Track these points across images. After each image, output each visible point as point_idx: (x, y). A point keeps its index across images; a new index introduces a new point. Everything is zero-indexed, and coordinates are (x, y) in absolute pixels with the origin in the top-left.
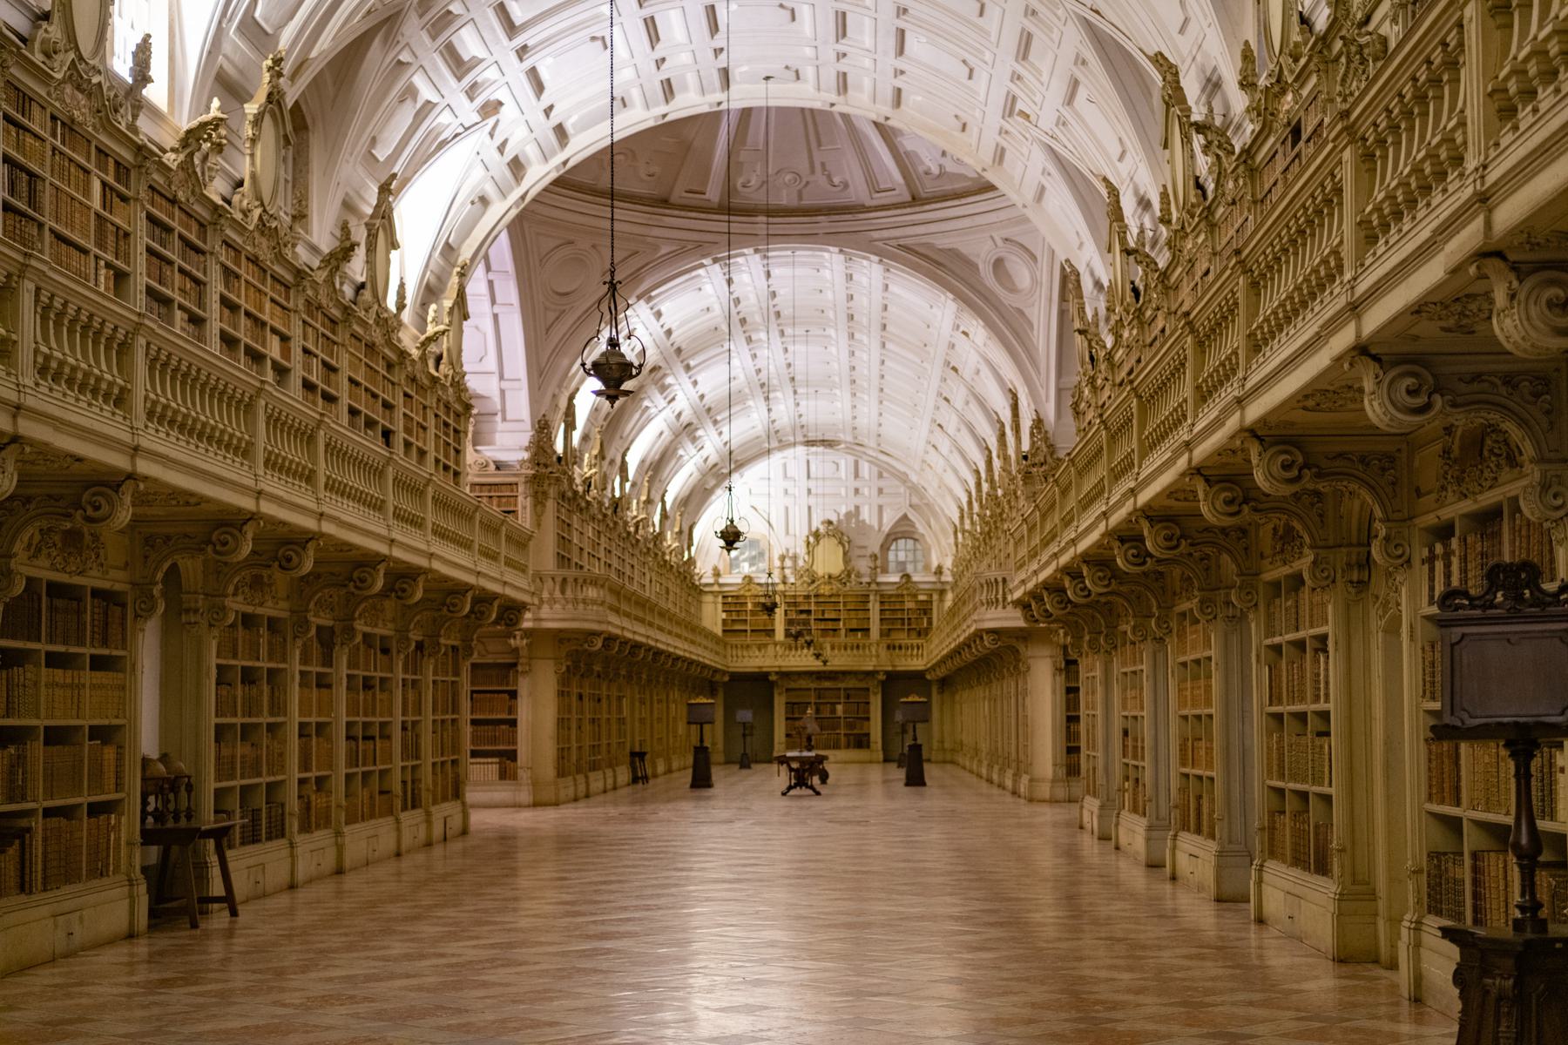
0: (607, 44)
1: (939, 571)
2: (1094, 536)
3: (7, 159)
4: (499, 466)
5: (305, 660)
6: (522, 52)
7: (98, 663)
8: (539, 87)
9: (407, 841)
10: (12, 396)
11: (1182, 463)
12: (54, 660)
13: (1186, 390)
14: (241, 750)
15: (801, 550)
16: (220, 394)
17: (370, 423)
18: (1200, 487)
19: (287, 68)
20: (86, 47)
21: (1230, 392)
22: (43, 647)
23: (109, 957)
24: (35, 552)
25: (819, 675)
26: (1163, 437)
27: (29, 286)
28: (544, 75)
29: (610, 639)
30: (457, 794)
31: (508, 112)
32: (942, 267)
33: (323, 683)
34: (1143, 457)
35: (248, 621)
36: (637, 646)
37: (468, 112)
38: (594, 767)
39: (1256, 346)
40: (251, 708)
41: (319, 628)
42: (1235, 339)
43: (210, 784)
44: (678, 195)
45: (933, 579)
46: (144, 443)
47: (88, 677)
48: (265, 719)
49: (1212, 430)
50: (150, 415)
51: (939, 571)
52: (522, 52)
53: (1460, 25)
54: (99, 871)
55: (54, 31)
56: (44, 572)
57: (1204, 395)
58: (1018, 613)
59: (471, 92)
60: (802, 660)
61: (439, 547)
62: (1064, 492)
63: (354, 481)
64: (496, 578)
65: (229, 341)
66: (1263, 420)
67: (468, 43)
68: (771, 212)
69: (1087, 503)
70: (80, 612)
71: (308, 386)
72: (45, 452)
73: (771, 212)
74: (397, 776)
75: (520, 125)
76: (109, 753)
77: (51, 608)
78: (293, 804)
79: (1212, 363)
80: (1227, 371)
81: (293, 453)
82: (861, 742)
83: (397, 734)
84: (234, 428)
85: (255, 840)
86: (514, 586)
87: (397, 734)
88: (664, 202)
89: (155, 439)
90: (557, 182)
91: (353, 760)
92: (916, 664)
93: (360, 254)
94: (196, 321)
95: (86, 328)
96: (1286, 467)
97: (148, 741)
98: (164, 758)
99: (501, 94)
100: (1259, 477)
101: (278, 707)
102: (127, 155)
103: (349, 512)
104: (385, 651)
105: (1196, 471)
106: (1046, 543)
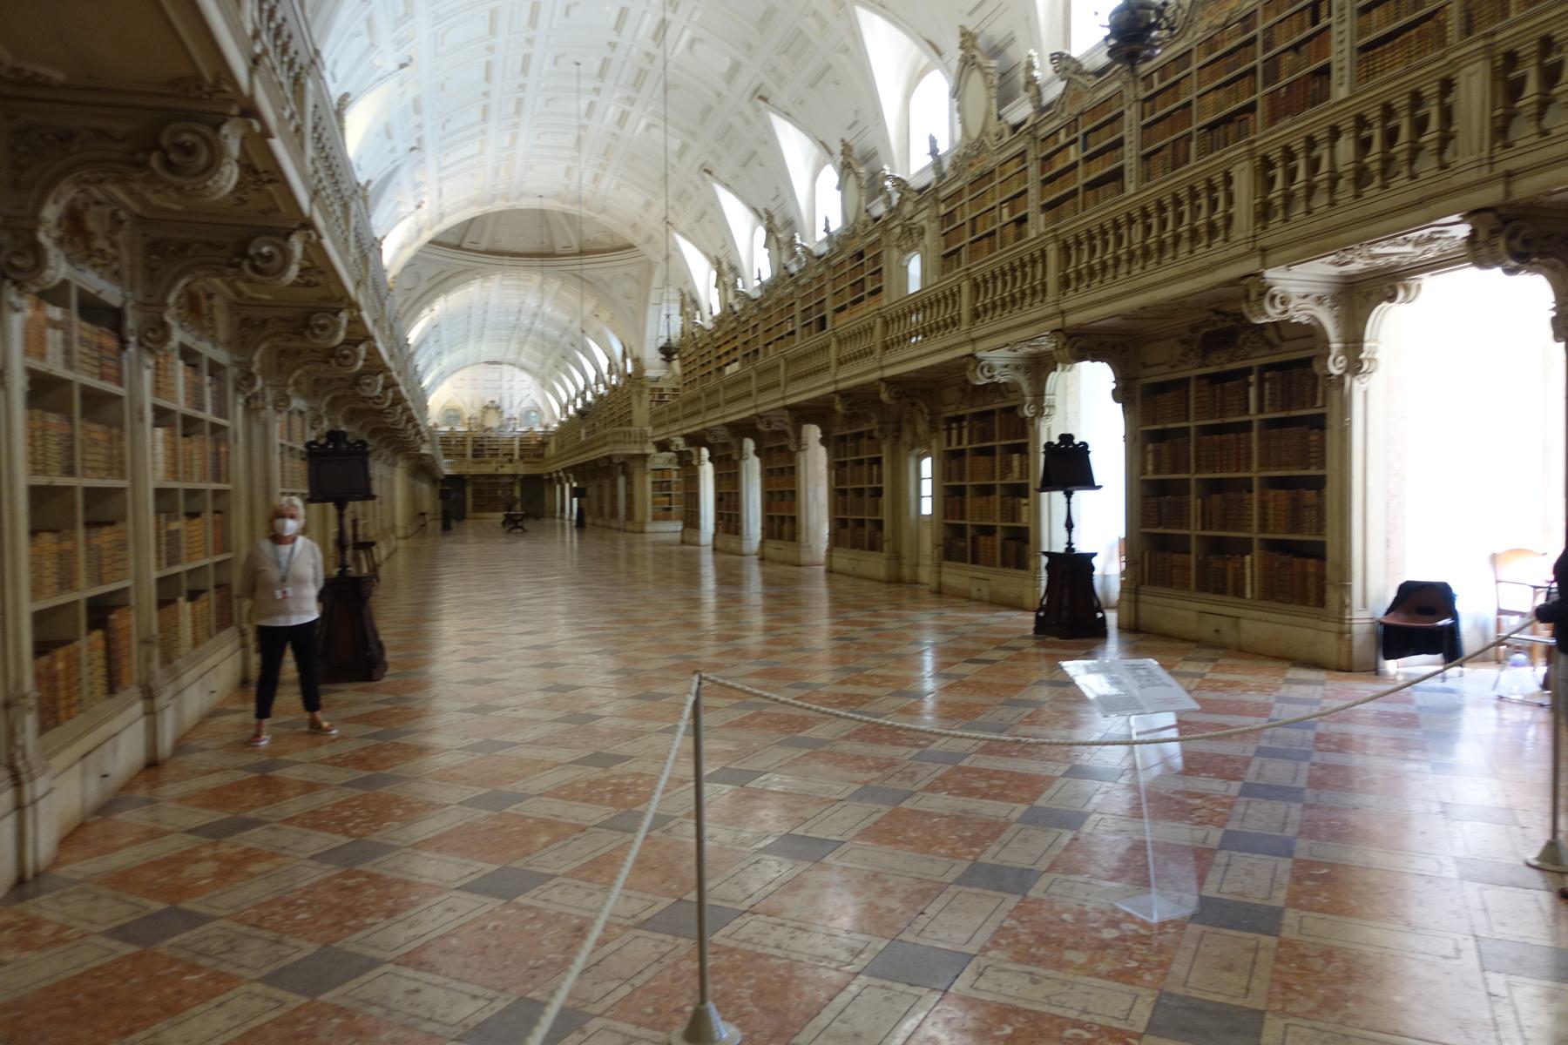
6: (441, 179)
8: (440, 195)
11: (831, 389)
15: (477, 414)
18: (837, 399)
31: (425, 206)
32: (586, 283)
39: (886, 347)
49: (853, 376)
52: (441, 179)
53: (1043, 252)
57: (840, 363)
59: (415, 197)
75: (424, 215)
79: (849, 349)
88: (458, 247)
90: (432, 242)
92: (537, 471)
99: (425, 199)
100: (884, 396)
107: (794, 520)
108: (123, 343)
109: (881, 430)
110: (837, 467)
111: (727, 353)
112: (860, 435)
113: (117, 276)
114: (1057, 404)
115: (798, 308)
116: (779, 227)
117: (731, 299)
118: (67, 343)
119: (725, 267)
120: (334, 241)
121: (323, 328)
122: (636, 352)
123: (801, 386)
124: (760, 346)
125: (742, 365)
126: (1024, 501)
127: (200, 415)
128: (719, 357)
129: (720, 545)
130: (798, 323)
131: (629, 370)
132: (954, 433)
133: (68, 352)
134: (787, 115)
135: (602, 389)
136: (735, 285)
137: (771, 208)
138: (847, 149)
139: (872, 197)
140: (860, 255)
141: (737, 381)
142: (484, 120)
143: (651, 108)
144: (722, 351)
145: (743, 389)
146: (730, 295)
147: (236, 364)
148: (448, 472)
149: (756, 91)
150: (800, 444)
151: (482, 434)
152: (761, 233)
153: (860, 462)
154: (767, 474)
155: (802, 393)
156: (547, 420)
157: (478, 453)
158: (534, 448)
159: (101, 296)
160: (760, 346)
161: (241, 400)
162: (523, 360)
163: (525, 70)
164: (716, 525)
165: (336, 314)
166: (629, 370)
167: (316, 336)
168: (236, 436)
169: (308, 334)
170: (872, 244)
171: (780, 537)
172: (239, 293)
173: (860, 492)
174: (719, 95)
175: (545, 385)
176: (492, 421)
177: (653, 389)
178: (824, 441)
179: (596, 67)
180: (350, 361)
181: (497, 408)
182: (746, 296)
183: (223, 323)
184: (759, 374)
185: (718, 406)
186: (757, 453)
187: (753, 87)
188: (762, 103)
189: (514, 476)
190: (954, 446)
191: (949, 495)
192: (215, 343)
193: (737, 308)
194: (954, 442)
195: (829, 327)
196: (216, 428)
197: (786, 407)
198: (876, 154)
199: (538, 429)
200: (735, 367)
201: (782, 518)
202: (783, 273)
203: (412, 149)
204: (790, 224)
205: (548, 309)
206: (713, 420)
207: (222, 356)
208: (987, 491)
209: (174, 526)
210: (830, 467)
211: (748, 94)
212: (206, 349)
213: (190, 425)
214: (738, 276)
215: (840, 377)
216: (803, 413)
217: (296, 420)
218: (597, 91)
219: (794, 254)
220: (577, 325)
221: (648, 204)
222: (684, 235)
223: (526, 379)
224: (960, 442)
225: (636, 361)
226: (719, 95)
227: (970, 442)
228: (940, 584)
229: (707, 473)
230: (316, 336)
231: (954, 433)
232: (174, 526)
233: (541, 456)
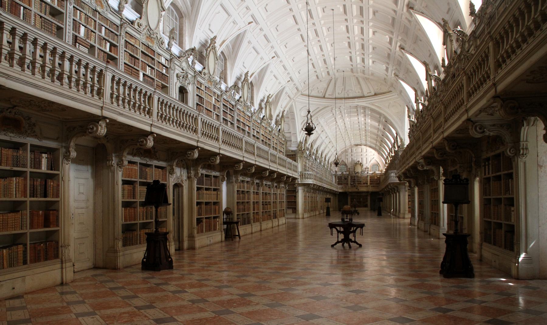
1: (381, 171)
2: (413, 163)
3: (197, 95)
4: (292, 151)
5: (254, 189)
7: (215, 190)
9: (274, 225)
10: (197, 139)
11: (431, 146)
12: (207, 189)
13: (432, 131)
14: (241, 207)
16: (236, 137)
17: (266, 143)
18: (435, 151)
19: (249, 75)
20: (211, 73)
21: (441, 130)
22: (204, 187)
23: (217, 245)
24: (203, 168)
26: (427, 141)
27: (200, 118)
29: (314, 185)
30: (284, 216)
33: (257, 193)
34: (423, 145)
35: (243, 181)
36: (320, 186)
38: (312, 211)
40: (244, 198)
41: (257, 183)
42: (442, 119)
43: (236, 213)
46: (221, 147)
47: (213, 192)
48: (246, 201)
49: (437, 139)
50: (223, 142)
51: (381, 171)
54: (215, 230)
55: (206, 71)
56: (204, 172)
57: (435, 132)
58: (397, 179)
60: (355, 190)
61: (279, 167)
62: (407, 154)
63: (262, 154)
64: (290, 173)
65: (238, 127)
66: (448, 137)
68: (345, 98)
69: (411, 156)
70: (211, 180)
71: (254, 136)
72: (203, 149)
73: (345, 98)
74: (272, 212)
76: (217, 207)
77: (206, 180)
78: (252, 217)
79: (437, 125)
80: (440, 126)
81: (250, 149)
82: (366, 206)
83: (272, 203)
84: (238, 144)
85: (245, 224)
86: (296, 175)
87: (272, 203)
88: (324, 97)
89: (223, 146)
91: (263, 209)
93: (263, 111)
94: (232, 124)
95: (210, 126)
96: (453, 146)
97: (224, 206)
98: (227, 208)
100: (447, 148)
101: (249, 199)
102: (219, 93)
103: (261, 160)
104: (269, 188)
105: (433, 148)
106: (403, 164)
109: (460, 167)
114: (529, 147)
119: (419, 93)
122: (402, 136)
126: (512, 209)
131: (399, 144)
132: (487, 167)
134: (422, 14)
135: (393, 154)
143: (371, 24)
148: (340, 191)
149: (408, 5)
155: (426, 149)
158: (376, 180)
162: (369, 143)
166: (399, 144)
169: (87, 132)
174: (395, 11)
176: (358, 169)
179: (342, 10)
188: (411, 11)
189: (368, 192)
190: (487, 176)
191: (485, 203)
194: (487, 174)
199: (377, 172)
205: (369, 121)
208: (499, 200)
220: (381, 127)
221: (387, 69)
222: (403, 80)
223: (373, 151)
224: (489, 173)
225: (401, 140)
226: (395, 11)
227: (492, 173)
228: (481, 256)
229: (416, 189)
231: (487, 167)
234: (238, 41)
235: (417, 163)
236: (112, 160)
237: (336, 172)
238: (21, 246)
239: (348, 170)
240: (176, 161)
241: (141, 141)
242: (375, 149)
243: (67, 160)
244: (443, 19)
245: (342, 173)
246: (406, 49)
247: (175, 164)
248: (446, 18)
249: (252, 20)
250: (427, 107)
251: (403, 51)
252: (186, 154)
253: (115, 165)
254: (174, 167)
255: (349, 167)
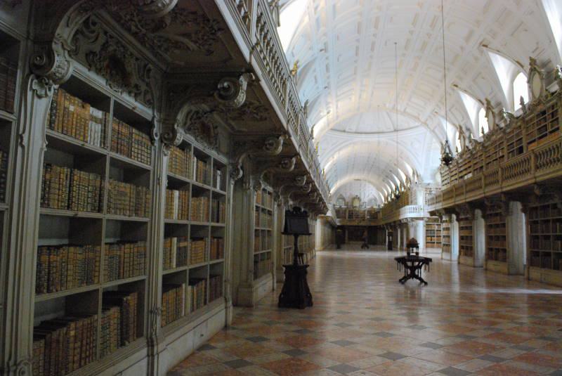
0: (350, 98)
6: (337, 101)
11: (533, 181)
25: (356, 226)
28: (339, 106)
31: (331, 112)
34: (503, 180)
37: (325, 113)
44: (347, 130)
45: (377, 207)
51: (379, 206)
57: (537, 168)
67: (329, 100)
75: (331, 116)
79: (543, 161)
88: (344, 131)
90: (332, 129)
105: (535, 183)
107: (505, 251)
108: (152, 140)
110: (532, 224)
111: (466, 169)
112: (545, 208)
113: (149, 103)
115: (505, 145)
116: (492, 107)
117: (467, 143)
118: (104, 131)
119: (464, 129)
120: (266, 82)
121: (271, 145)
123: (512, 181)
124: (484, 164)
125: (474, 174)
127: (206, 186)
128: (461, 172)
129: (462, 261)
130: (506, 151)
133: (104, 138)
134: (498, 52)
136: (470, 137)
137: (489, 98)
138: (533, 62)
139: (549, 83)
140: (544, 113)
141: (471, 182)
142: (355, 74)
144: (462, 169)
145: (477, 185)
146: (467, 141)
147: (232, 164)
148: (338, 224)
149: (481, 43)
150: (508, 211)
151: (352, 209)
152: (483, 112)
153: (548, 221)
154: (489, 227)
156: (378, 204)
157: (351, 216)
158: (374, 214)
159: (135, 111)
160: (484, 164)
161: (233, 182)
163: (372, 49)
164: (460, 252)
165: (278, 138)
167: (267, 149)
168: (229, 200)
169: (264, 148)
170: (553, 107)
171: (496, 259)
172: (233, 128)
173: (547, 238)
175: (379, 189)
176: (356, 204)
177: (426, 189)
178: (524, 210)
180: (289, 165)
181: (359, 198)
182: (476, 141)
183: (224, 141)
184: (485, 177)
185: (463, 194)
186: (484, 217)
187: (480, 40)
188: (484, 48)
189: (365, 227)
192: (218, 150)
193: (470, 147)
195: (525, 151)
196: (217, 196)
197: (502, 193)
198: (549, 62)
199: (375, 207)
200: (470, 175)
201: (498, 250)
202: (496, 128)
203: (326, 88)
204: (499, 104)
206: (460, 200)
207: (223, 160)
209: (182, 244)
210: (527, 223)
211: (477, 45)
212: (213, 154)
213: (198, 192)
214: (470, 133)
215: (537, 174)
216: (512, 195)
217: (267, 197)
218: (404, 55)
219: (503, 117)
223: (371, 186)
226: (462, 48)
230: (267, 149)
232: (182, 244)
233: (376, 218)
234: (307, 67)
235: (486, 198)
236: (249, 183)
237: (334, 205)
238: (203, 282)
239: (346, 204)
240: (283, 186)
241: (285, 163)
242: (374, 185)
243: (233, 178)
244: (531, 59)
245: (340, 207)
246: (459, 86)
247: (280, 190)
248: (533, 57)
249: (323, 48)
250: (482, 144)
251: (455, 88)
252: (295, 180)
253: (252, 188)
254: (279, 194)
255: (347, 200)
